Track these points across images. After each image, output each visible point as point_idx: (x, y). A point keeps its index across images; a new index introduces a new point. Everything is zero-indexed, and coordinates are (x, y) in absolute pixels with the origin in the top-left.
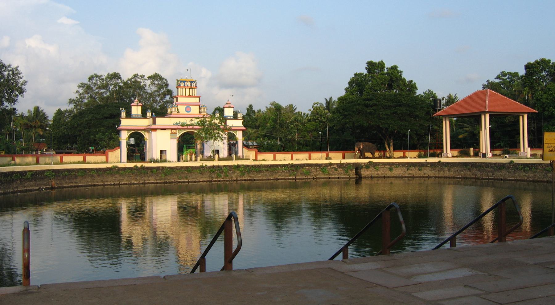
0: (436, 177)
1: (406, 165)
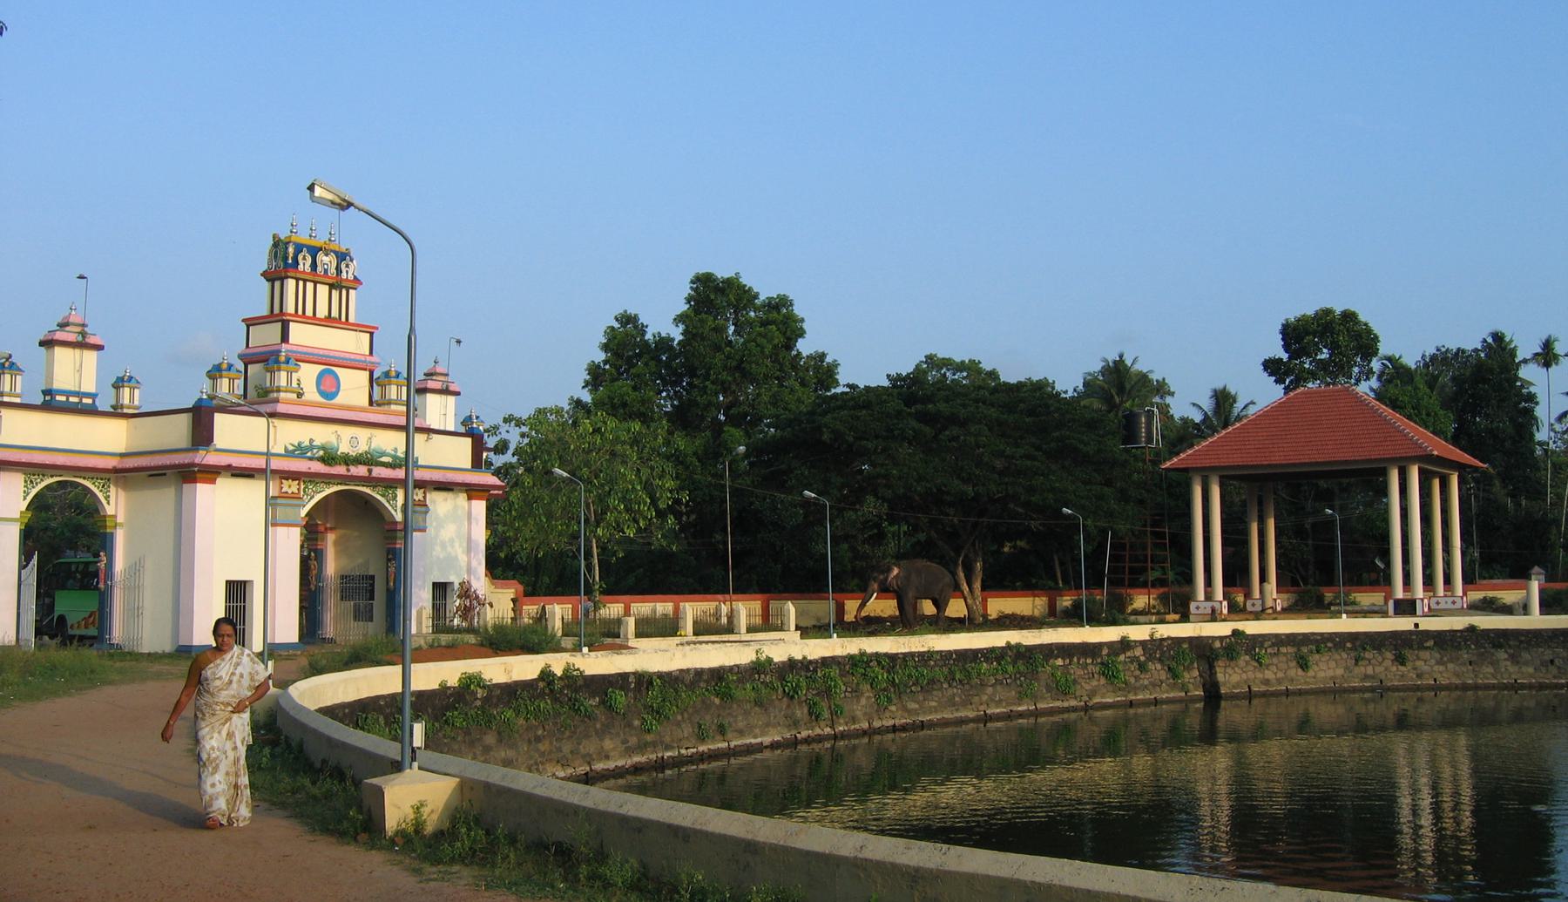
0: (1465, 687)
1: (1349, 645)
